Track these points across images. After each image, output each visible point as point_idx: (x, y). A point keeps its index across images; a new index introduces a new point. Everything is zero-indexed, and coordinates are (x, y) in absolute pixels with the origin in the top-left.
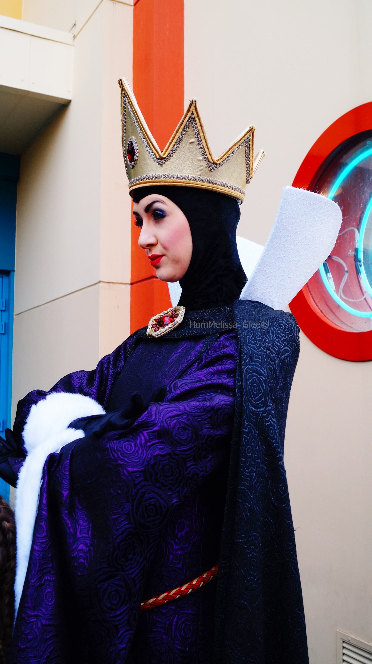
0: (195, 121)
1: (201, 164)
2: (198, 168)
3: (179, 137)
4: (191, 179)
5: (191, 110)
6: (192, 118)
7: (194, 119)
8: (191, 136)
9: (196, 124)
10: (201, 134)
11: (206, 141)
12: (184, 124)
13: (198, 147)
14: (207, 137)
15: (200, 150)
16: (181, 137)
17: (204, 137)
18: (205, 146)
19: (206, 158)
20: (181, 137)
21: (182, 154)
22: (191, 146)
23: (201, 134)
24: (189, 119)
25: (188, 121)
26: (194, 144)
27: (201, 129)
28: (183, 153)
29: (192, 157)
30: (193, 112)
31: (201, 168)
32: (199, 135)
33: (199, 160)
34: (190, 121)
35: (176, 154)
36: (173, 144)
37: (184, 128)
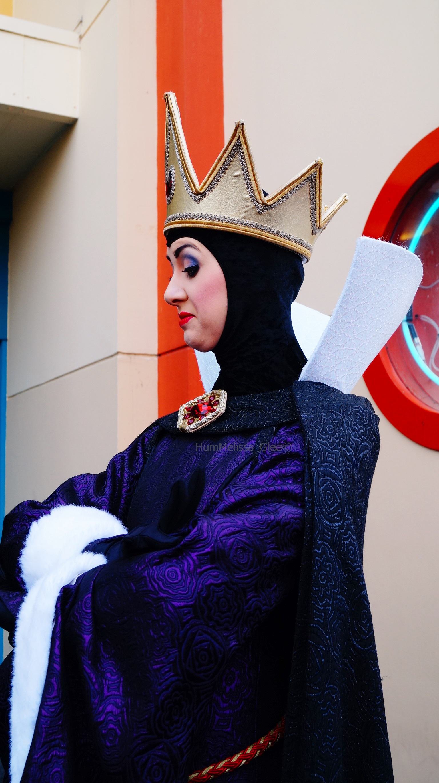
2: (243, 208)
5: (237, 134)
6: (238, 145)
7: (240, 146)
8: (236, 168)
9: (243, 153)
10: (249, 166)
11: (254, 175)
12: (228, 152)
13: (244, 182)
14: (256, 170)
15: (246, 186)
16: (223, 168)
17: (253, 170)
18: (253, 182)
19: (252, 196)
20: (223, 168)
21: (224, 190)
22: (236, 180)
24: (234, 145)
28: (224, 188)
29: (235, 194)
30: (239, 137)
32: (246, 167)
33: (246, 199)
34: (236, 149)
35: (216, 190)
36: (213, 176)
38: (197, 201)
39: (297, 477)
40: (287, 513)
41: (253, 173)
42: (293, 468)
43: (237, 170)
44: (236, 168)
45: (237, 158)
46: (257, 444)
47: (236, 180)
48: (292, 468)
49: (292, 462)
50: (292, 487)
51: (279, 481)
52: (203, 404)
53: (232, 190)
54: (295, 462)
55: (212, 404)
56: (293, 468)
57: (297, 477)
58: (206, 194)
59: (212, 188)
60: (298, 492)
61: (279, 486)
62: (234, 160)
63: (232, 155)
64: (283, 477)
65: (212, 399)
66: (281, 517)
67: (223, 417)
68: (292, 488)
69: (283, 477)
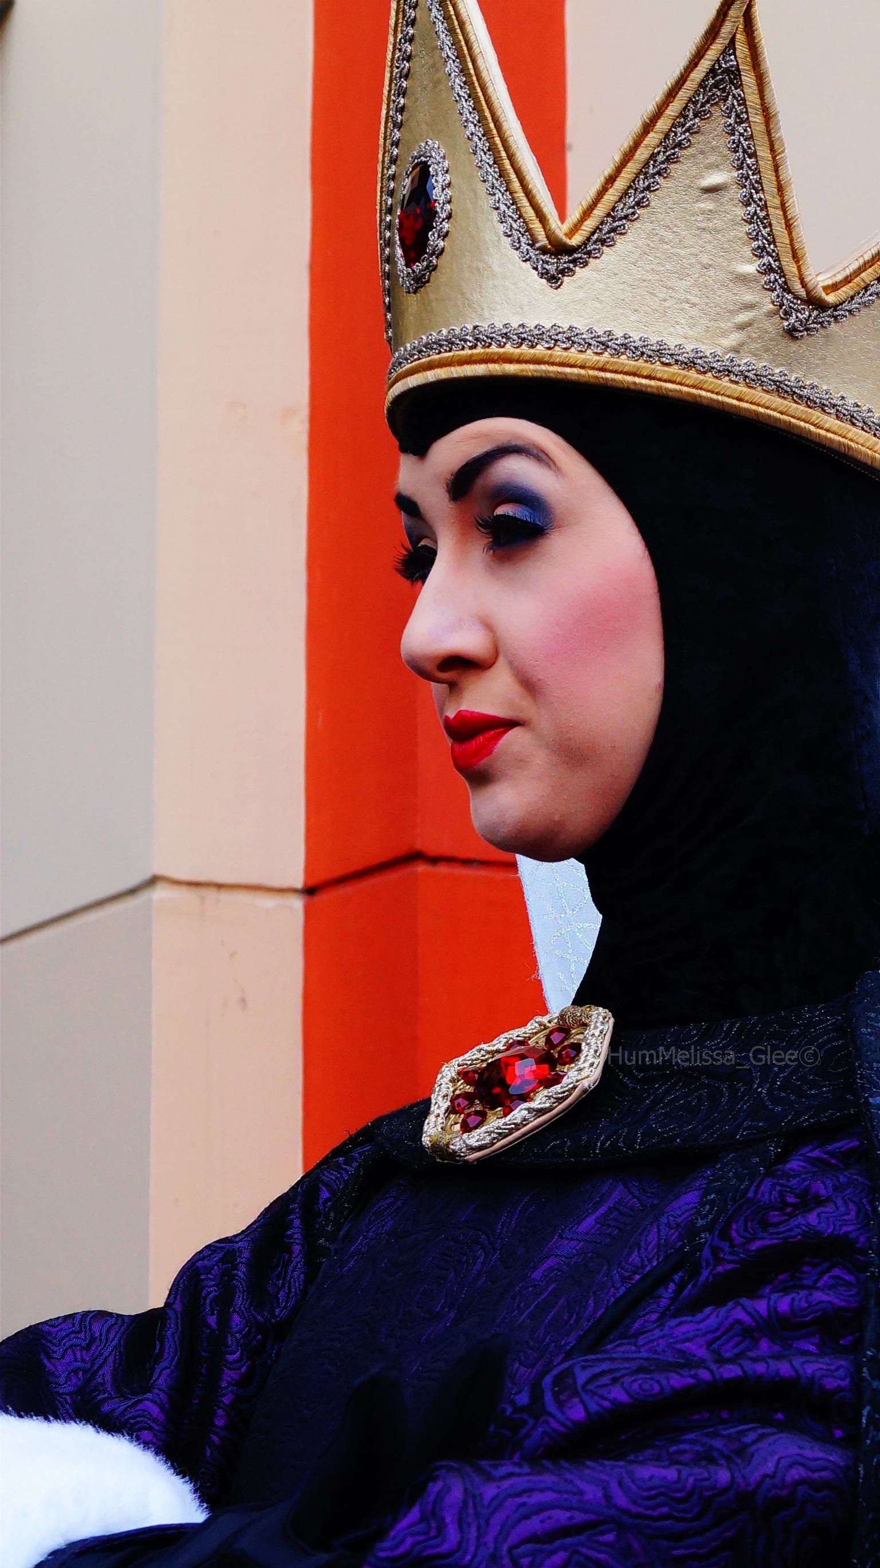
0: (740, 86)
1: (749, 297)
3: (653, 156)
4: (690, 364)
5: (726, 29)
6: (727, 71)
7: (735, 74)
8: (712, 159)
9: (743, 102)
10: (764, 152)
11: (780, 189)
12: (683, 95)
13: (740, 212)
14: (791, 170)
15: (748, 228)
16: (661, 158)
17: (776, 169)
18: (776, 214)
19: (770, 269)
20: (661, 158)
21: (662, 241)
24: (712, 72)
25: (702, 84)
26: (726, 196)
27: (762, 128)
28: (662, 232)
30: (733, 41)
31: (743, 317)
32: (754, 155)
34: (716, 86)
35: (630, 236)
36: (620, 184)
37: (683, 115)
38: (554, 279)
39: (833, 1329)
40: (784, 1462)
41: (778, 181)
42: (826, 1293)
44: (712, 159)
45: (718, 122)
46: (703, 1206)
48: (818, 1296)
49: (822, 1274)
50: (815, 1366)
51: (764, 1344)
52: (522, 1057)
53: (691, 241)
54: (836, 1272)
55: (557, 1053)
56: (826, 1293)
57: (833, 1329)
58: (589, 253)
59: (613, 230)
60: (831, 1383)
61: (766, 1362)
62: (706, 127)
63: (697, 109)
64: (781, 1329)
65: (556, 1038)
66: (757, 1475)
67: (590, 1103)
68: (810, 1369)
69: (781, 1329)
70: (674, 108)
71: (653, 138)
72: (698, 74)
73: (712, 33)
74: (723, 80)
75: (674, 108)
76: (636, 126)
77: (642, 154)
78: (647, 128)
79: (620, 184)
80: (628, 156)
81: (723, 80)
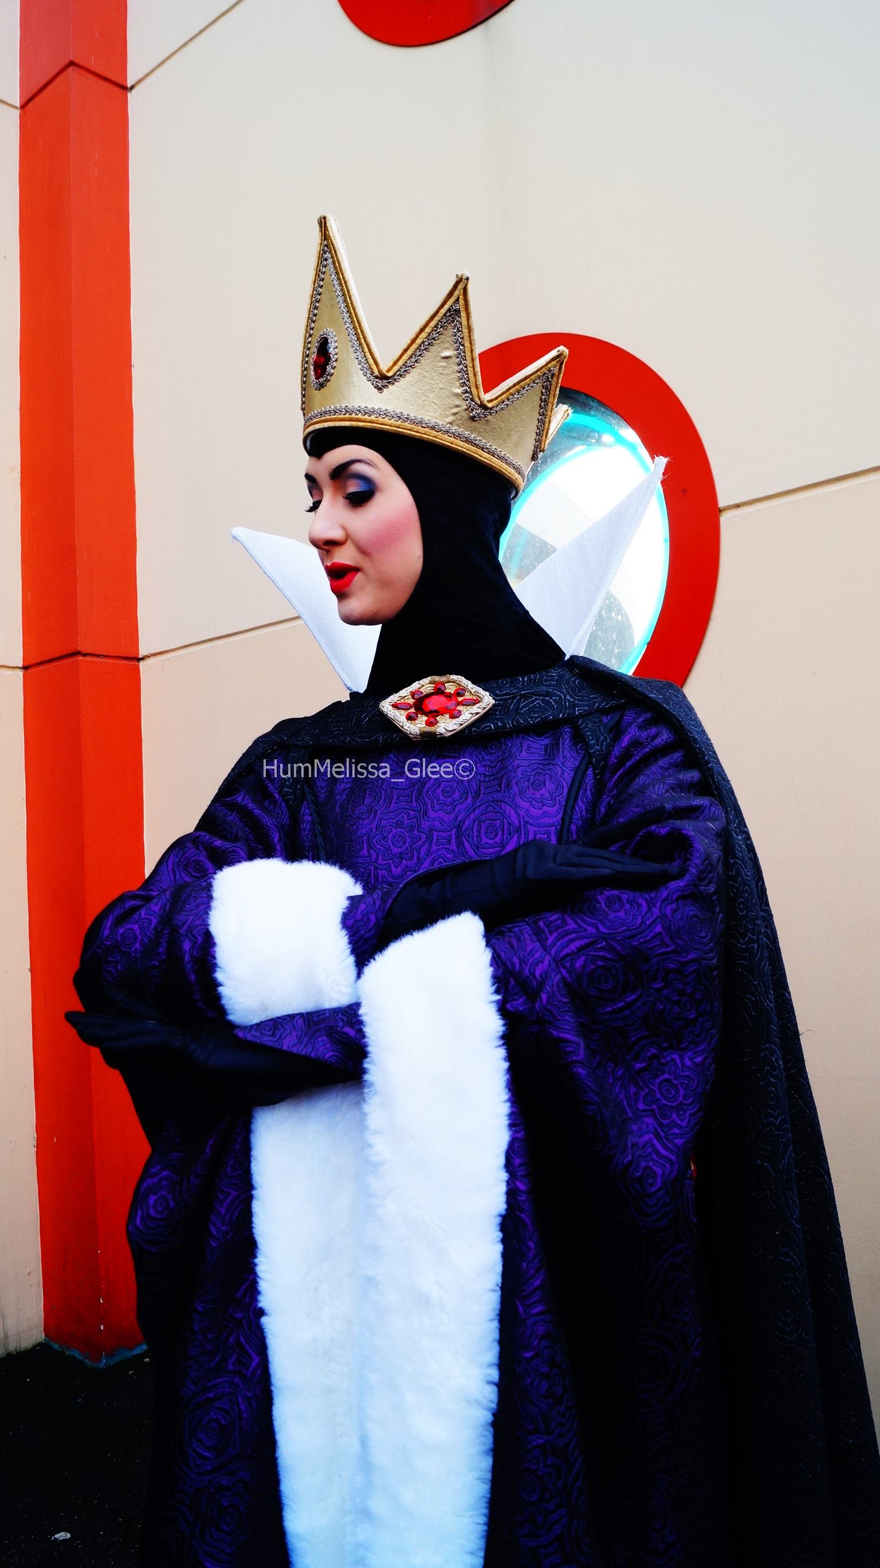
0: (460, 317)
1: (458, 403)
3: (423, 342)
4: (433, 428)
6: (455, 310)
7: (458, 312)
8: (446, 345)
9: (461, 323)
10: (467, 344)
12: (437, 318)
13: (457, 368)
19: (467, 392)
22: (444, 364)
23: (467, 344)
24: (449, 310)
25: (445, 315)
29: (441, 386)
30: (458, 300)
31: (455, 410)
33: (457, 395)
36: (409, 352)
37: (436, 326)
43: (446, 348)
44: (446, 345)
45: (451, 330)
47: (444, 364)
62: (445, 332)
63: (442, 325)
70: (433, 324)
71: (424, 335)
72: (443, 311)
73: (450, 294)
74: (453, 314)
75: (433, 324)
76: (417, 329)
77: (419, 341)
78: (422, 330)
79: (409, 352)
80: (413, 341)
81: (453, 314)
